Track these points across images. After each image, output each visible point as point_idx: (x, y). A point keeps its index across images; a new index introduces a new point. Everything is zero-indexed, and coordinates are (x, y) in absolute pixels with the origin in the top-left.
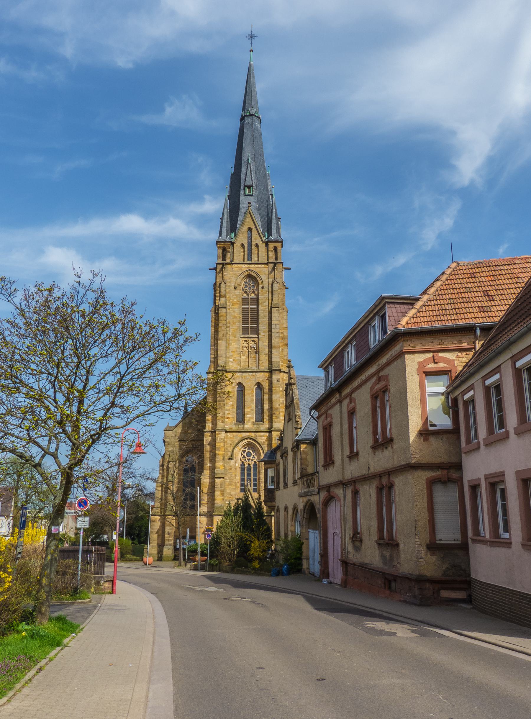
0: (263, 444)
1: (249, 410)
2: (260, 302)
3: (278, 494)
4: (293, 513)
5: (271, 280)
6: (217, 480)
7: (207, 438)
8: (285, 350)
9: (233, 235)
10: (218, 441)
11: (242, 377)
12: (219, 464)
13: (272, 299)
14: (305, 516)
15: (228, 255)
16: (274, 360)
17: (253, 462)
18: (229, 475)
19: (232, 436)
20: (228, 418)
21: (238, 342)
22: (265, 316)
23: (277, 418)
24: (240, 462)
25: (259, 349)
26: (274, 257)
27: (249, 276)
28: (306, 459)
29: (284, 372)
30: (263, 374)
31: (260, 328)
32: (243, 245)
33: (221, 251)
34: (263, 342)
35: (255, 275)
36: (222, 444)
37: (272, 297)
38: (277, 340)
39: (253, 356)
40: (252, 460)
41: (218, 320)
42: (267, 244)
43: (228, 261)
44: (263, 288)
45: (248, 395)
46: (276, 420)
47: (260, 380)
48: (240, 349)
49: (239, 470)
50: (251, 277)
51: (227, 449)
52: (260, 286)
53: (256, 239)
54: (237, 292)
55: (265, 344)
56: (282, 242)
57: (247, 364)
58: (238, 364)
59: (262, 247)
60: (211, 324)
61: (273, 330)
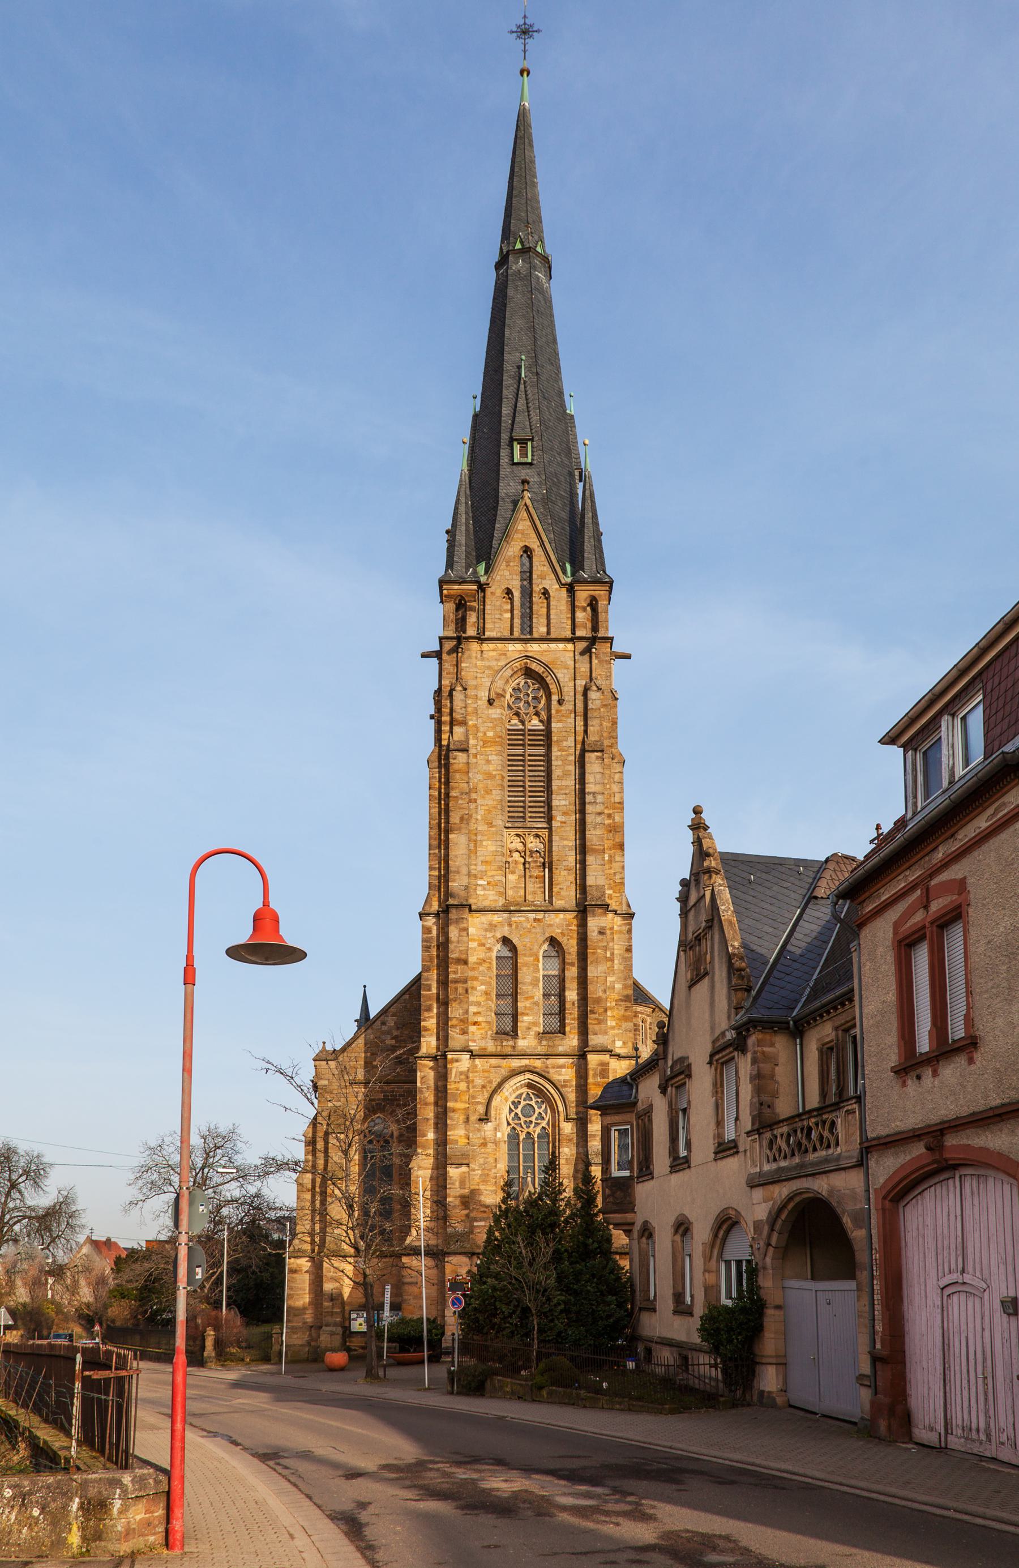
0: (563, 1086)
1: (528, 1004)
2: (554, 738)
3: (642, 1191)
4: (716, 1236)
5: (581, 683)
6: (453, 1172)
7: (426, 1074)
8: (618, 858)
9: (481, 568)
10: (453, 1076)
11: (510, 925)
12: (456, 1132)
13: (586, 732)
14: (774, 1242)
15: (472, 618)
16: (590, 881)
17: (538, 1130)
18: (481, 1161)
19: (486, 1066)
20: (475, 1023)
21: (499, 837)
22: (566, 774)
23: (600, 1022)
24: (506, 1130)
25: (550, 851)
26: (589, 625)
27: (528, 673)
28: (772, 1076)
29: (615, 912)
30: (561, 916)
31: (555, 803)
32: (509, 592)
33: (451, 606)
34: (562, 839)
35: (540, 669)
36: (463, 1086)
37: (586, 725)
38: (598, 832)
39: (536, 873)
40: (537, 1124)
41: (447, 783)
42: (571, 589)
43: (471, 632)
44: (560, 702)
45: (524, 969)
46: (596, 1027)
47: (556, 932)
48: (503, 855)
49: (504, 1148)
50: (535, 676)
51: (474, 1097)
52: (555, 698)
53: (545, 578)
54: (495, 712)
55: (565, 843)
56: (611, 584)
57: (522, 892)
58: (500, 894)
59: (560, 597)
60: (427, 792)
61: (589, 808)
